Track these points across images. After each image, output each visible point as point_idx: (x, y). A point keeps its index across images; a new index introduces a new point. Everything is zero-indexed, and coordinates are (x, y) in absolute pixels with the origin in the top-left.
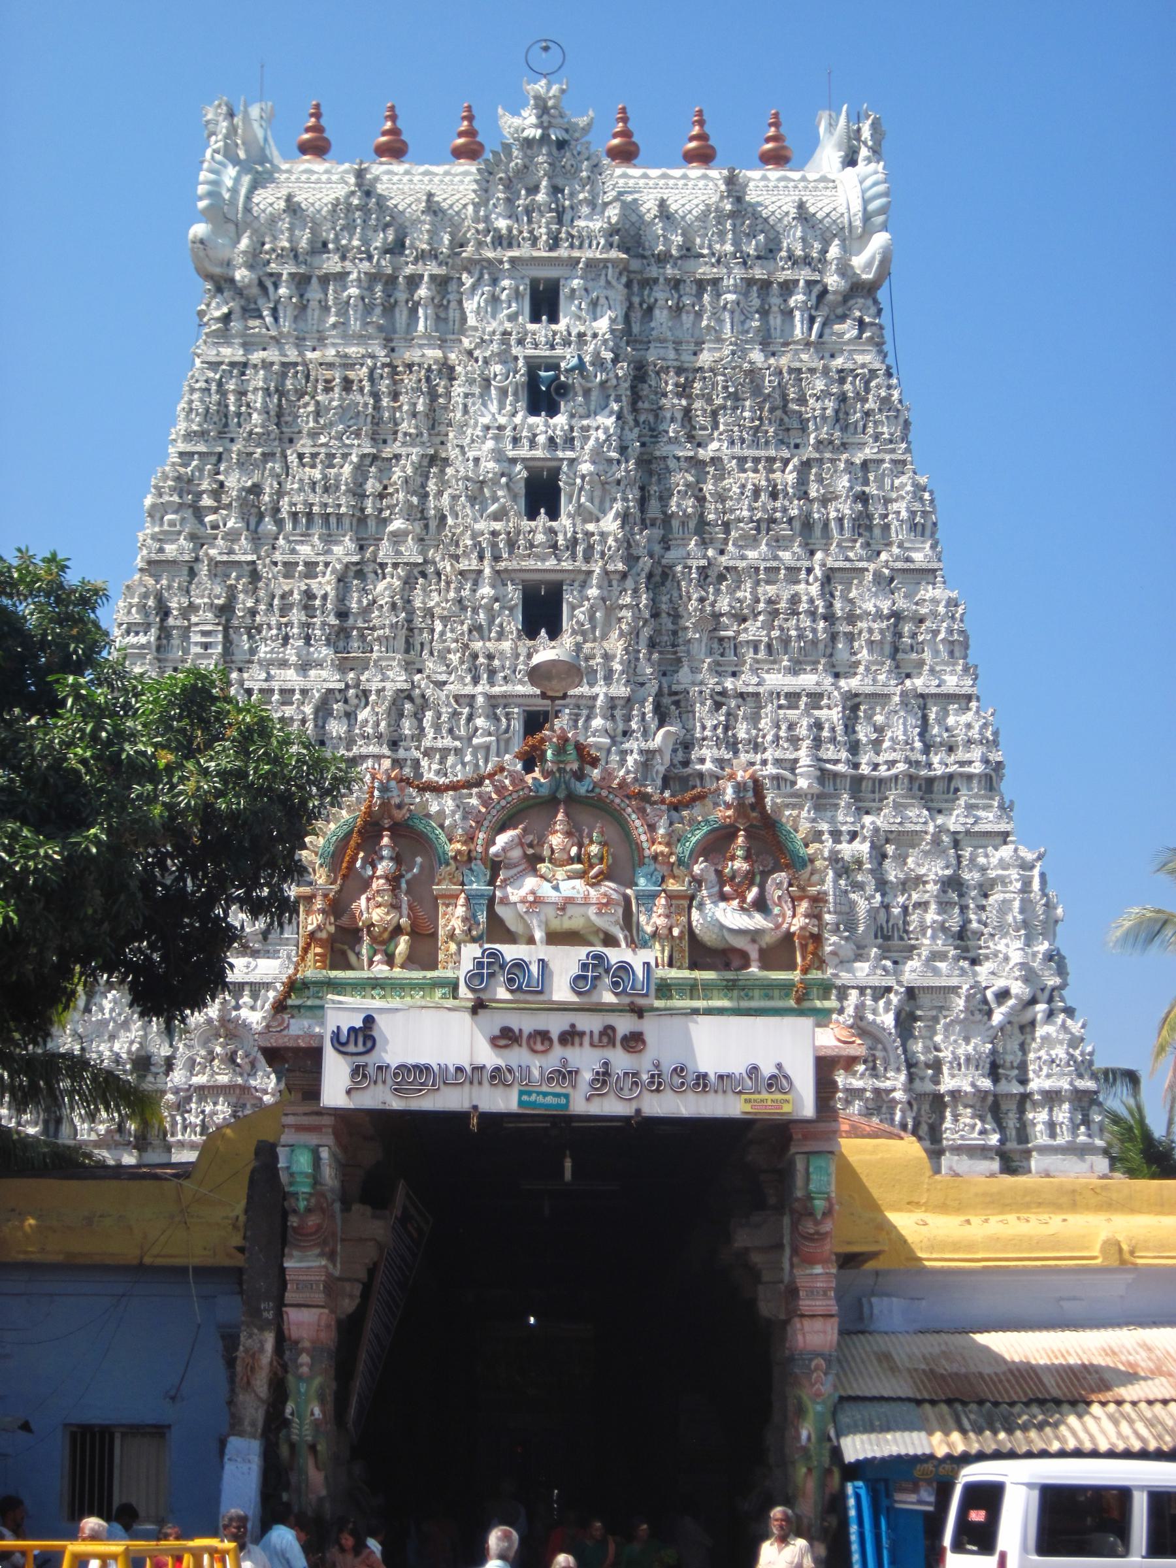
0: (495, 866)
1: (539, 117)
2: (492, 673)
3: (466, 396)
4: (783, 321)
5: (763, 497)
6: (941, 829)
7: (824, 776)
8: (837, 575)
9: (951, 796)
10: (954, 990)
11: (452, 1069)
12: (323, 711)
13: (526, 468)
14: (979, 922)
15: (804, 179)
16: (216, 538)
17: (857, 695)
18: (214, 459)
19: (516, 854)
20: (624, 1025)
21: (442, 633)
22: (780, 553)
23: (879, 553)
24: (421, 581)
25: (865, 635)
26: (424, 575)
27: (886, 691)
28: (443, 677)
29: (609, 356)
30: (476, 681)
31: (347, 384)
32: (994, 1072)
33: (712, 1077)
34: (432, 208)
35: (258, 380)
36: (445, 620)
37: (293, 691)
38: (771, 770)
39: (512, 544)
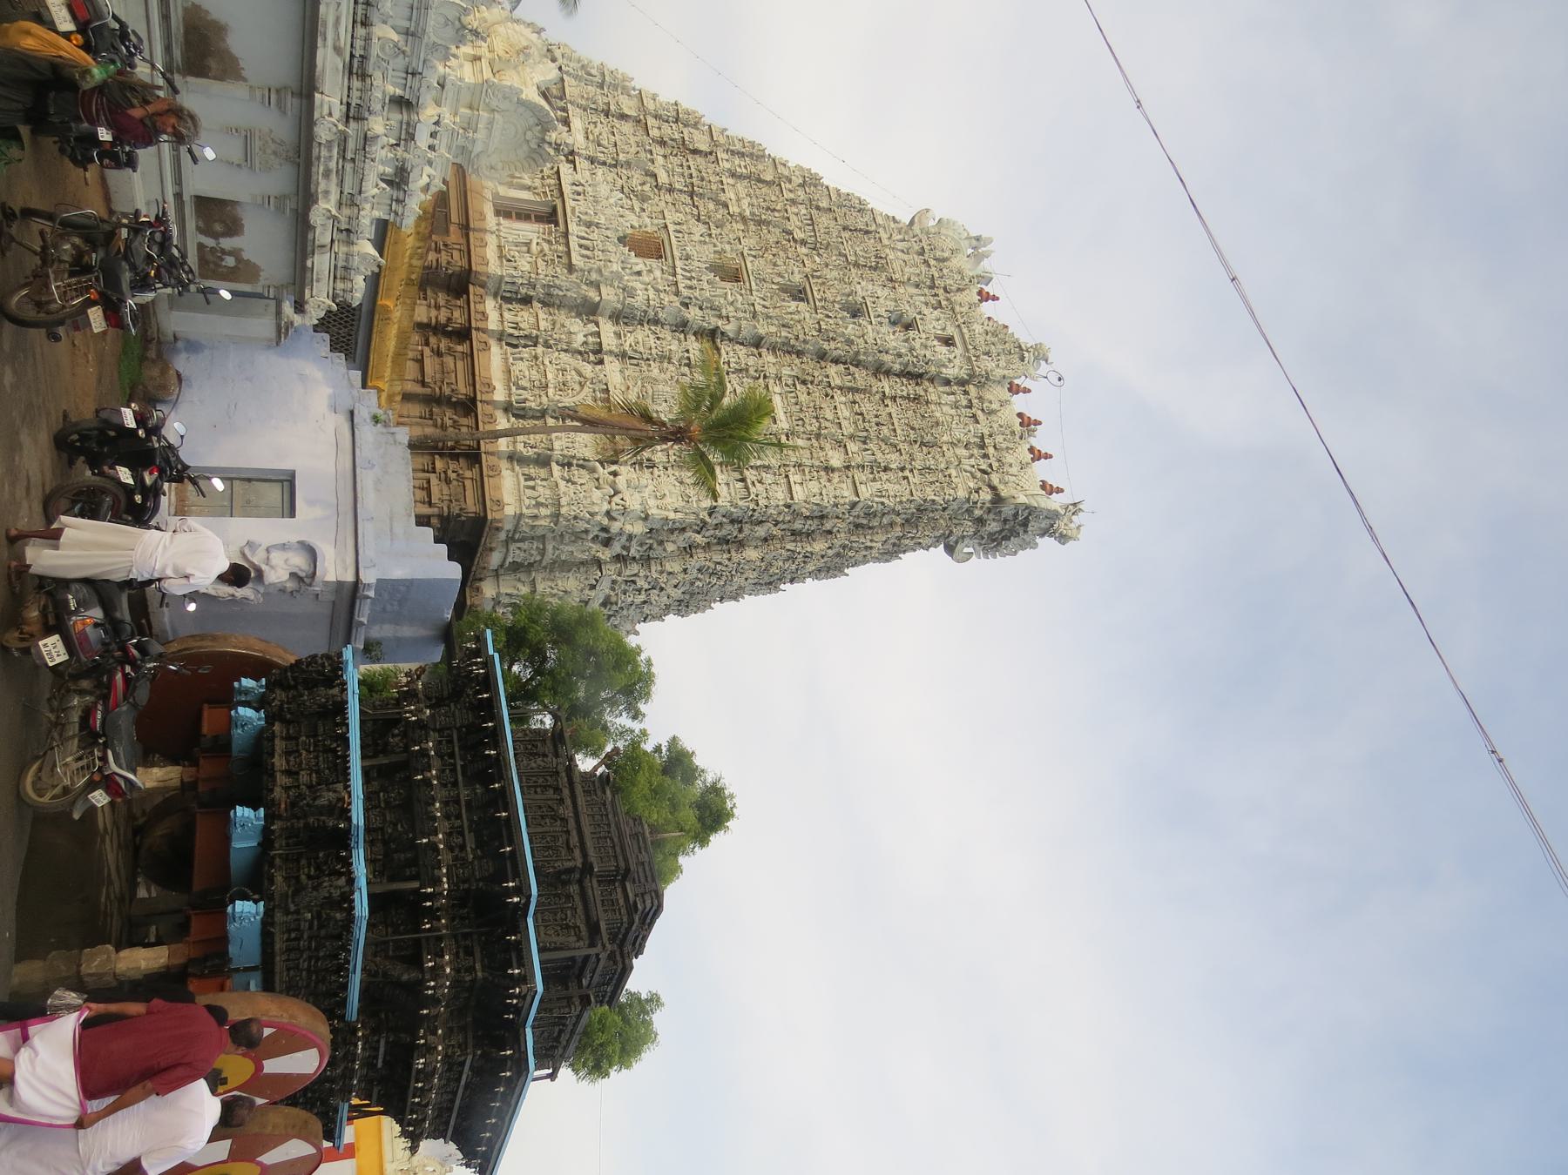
2: (755, 257)
8: (842, 449)
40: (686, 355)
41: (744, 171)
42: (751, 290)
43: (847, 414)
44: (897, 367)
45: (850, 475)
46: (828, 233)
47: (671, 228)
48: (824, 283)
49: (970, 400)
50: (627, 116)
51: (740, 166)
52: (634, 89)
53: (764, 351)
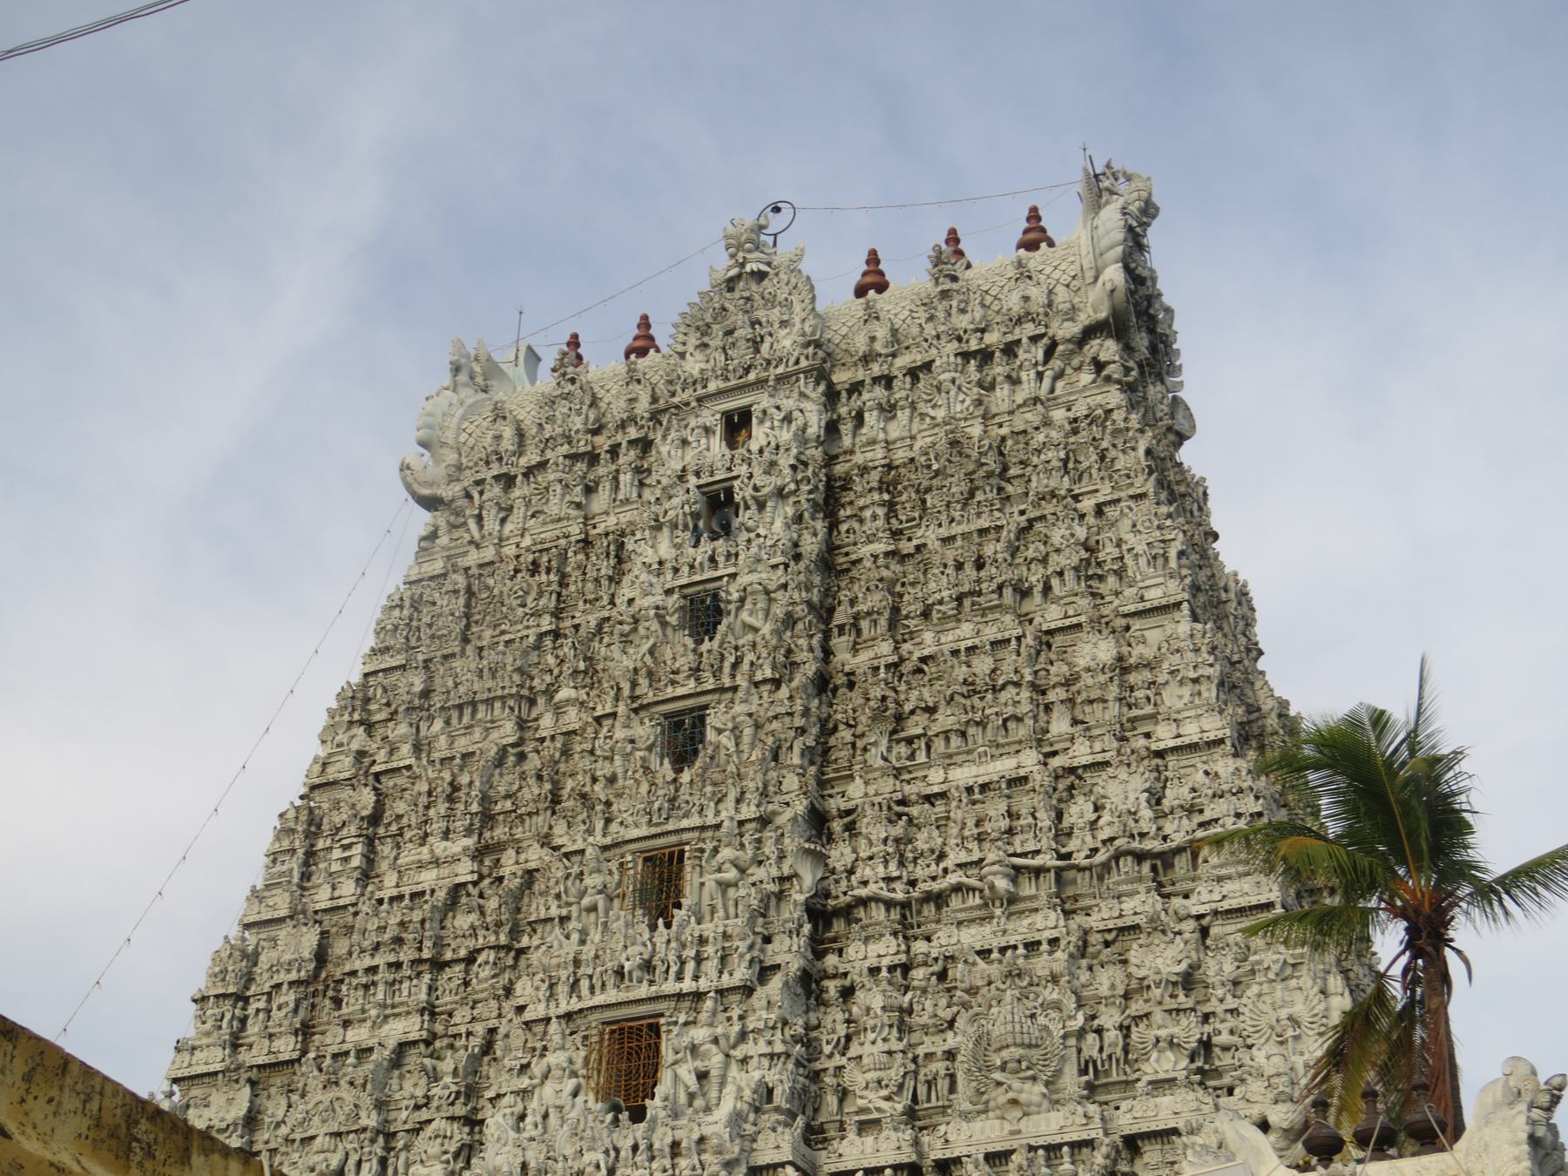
2: (608, 821)
8: (1058, 641)
38: (953, 879)
40: (884, 973)
41: (358, 849)
42: (703, 828)
43: (966, 629)
44: (820, 525)
45: (1123, 622)
46: (493, 673)
47: (565, 1004)
48: (650, 674)
49: (875, 380)
50: (250, 1110)
51: (346, 860)
52: (171, 1094)
53: (835, 804)
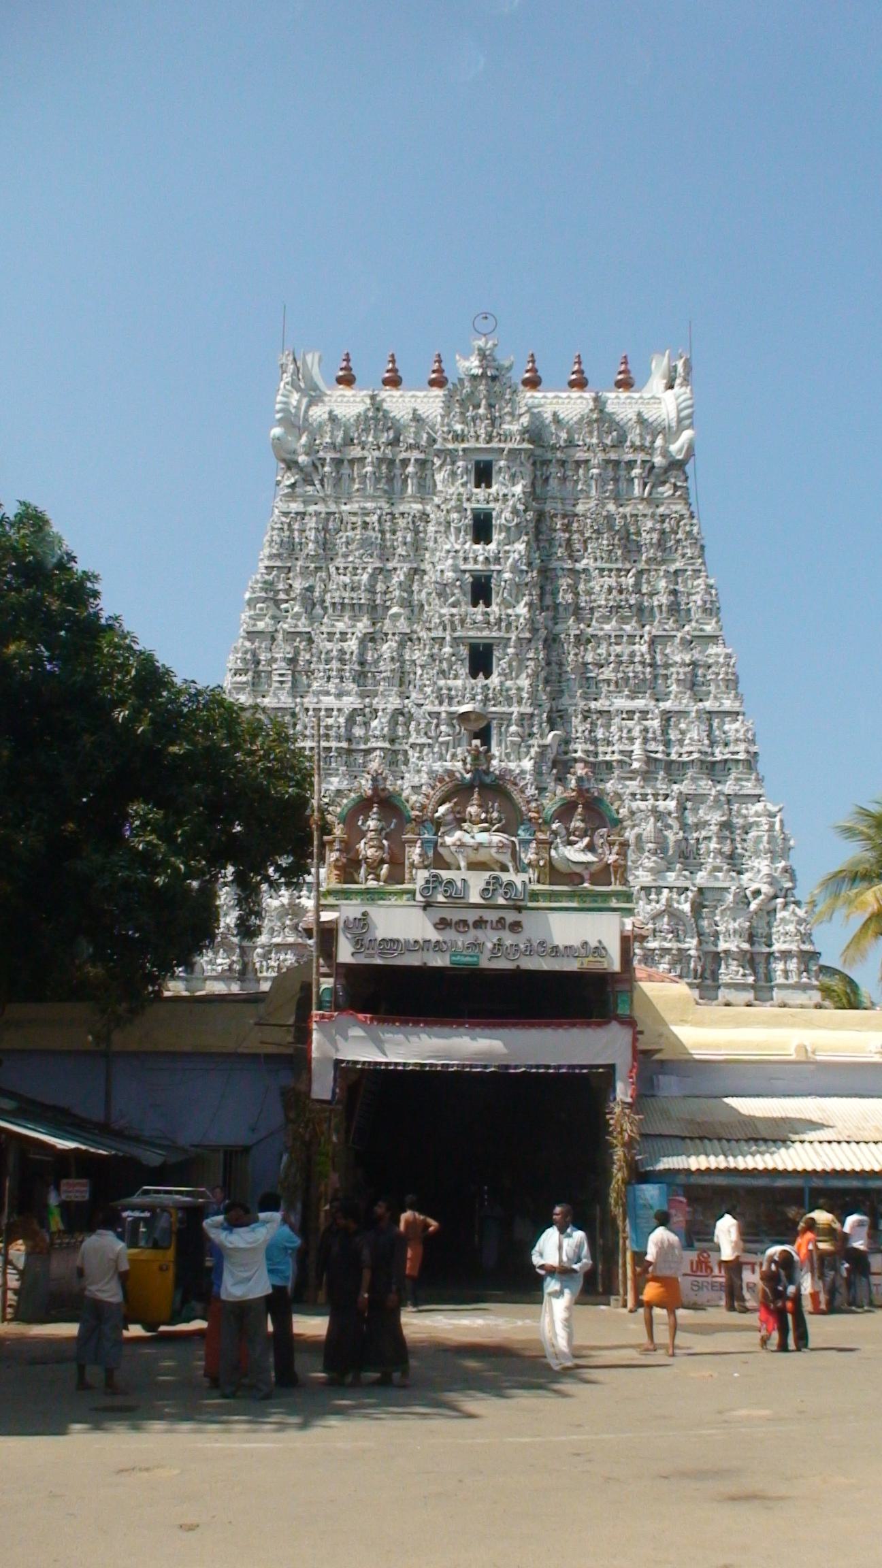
0: (438, 824)
1: (481, 361)
2: (451, 698)
3: (436, 532)
4: (628, 485)
5: (615, 592)
6: (720, 793)
7: (650, 760)
9: (726, 773)
10: (726, 889)
11: (412, 942)
12: (351, 720)
13: (472, 576)
14: (743, 849)
15: (641, 398)
16: (287, 618)
17: (669, 712)
18: (286, 571)
19: (450, 817)
20: (511, 917)
21: (421, 675)
22: (624, 627)
23: (684, 626)
24: (409, 643)
25: (674, 676)
26: (411, 640)
27: (687, 709)
28: (421, 702)
29: (521, 507)
30: (441, 703)
31: (365, 525)
32: (751, 939)
33: (561, 947)
34: (417, 418)
35: (311, 523)
36: (422, 667)
37: (332, 710)
38: (617, 757)
39: (462, 622)
